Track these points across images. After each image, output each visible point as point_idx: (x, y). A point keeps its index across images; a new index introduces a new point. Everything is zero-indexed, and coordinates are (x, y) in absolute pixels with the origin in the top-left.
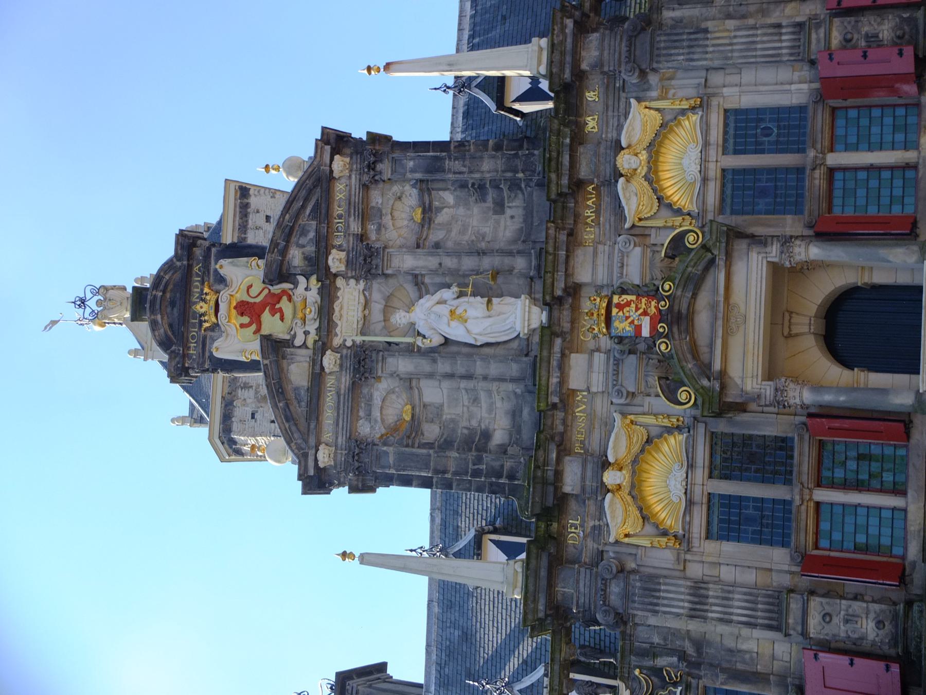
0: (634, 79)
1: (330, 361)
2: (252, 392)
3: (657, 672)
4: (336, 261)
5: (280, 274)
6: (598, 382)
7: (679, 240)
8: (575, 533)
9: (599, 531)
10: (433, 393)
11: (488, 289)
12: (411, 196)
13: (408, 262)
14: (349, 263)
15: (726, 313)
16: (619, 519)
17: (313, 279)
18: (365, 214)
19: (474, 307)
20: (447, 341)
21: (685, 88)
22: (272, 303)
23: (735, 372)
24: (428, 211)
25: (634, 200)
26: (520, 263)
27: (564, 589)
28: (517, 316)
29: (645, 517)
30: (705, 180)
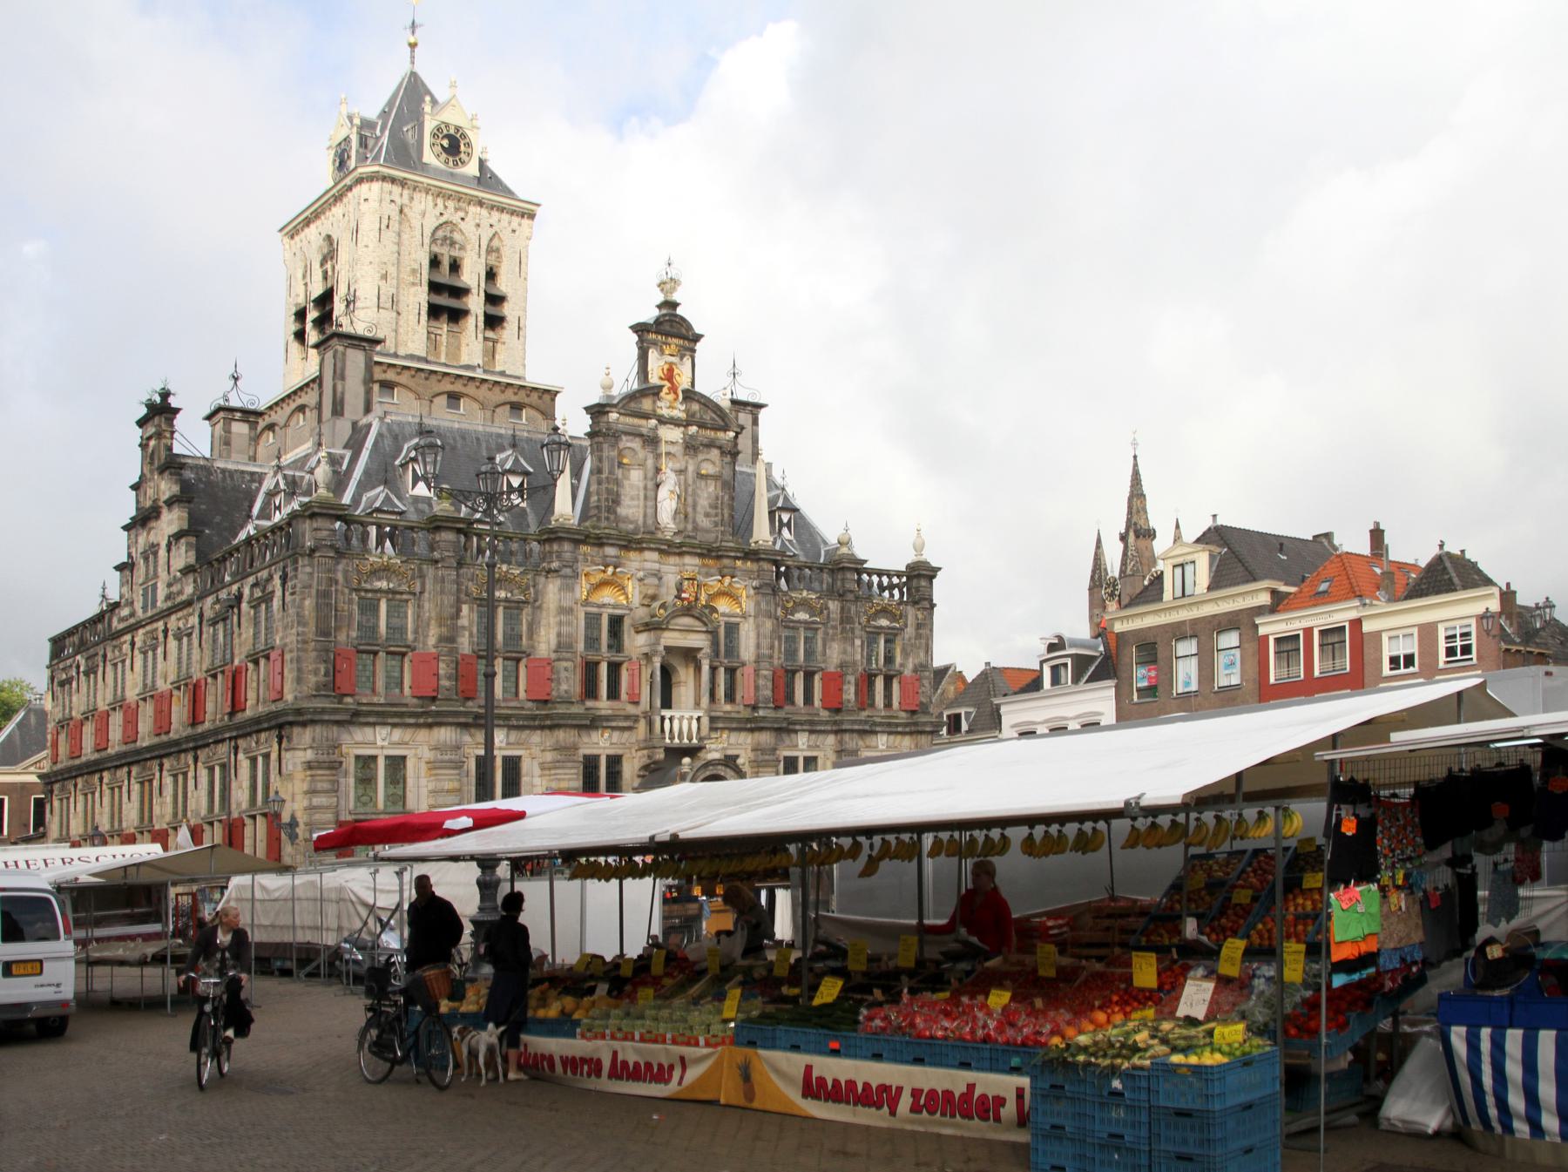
0: (755, 583)
2: (405, 200)
3: (528, 588)
6: (648, 565)
8: (584, 549)
21: (748, 605)
23: (667, 634)
25: (713, 583)
27: (567, 546)
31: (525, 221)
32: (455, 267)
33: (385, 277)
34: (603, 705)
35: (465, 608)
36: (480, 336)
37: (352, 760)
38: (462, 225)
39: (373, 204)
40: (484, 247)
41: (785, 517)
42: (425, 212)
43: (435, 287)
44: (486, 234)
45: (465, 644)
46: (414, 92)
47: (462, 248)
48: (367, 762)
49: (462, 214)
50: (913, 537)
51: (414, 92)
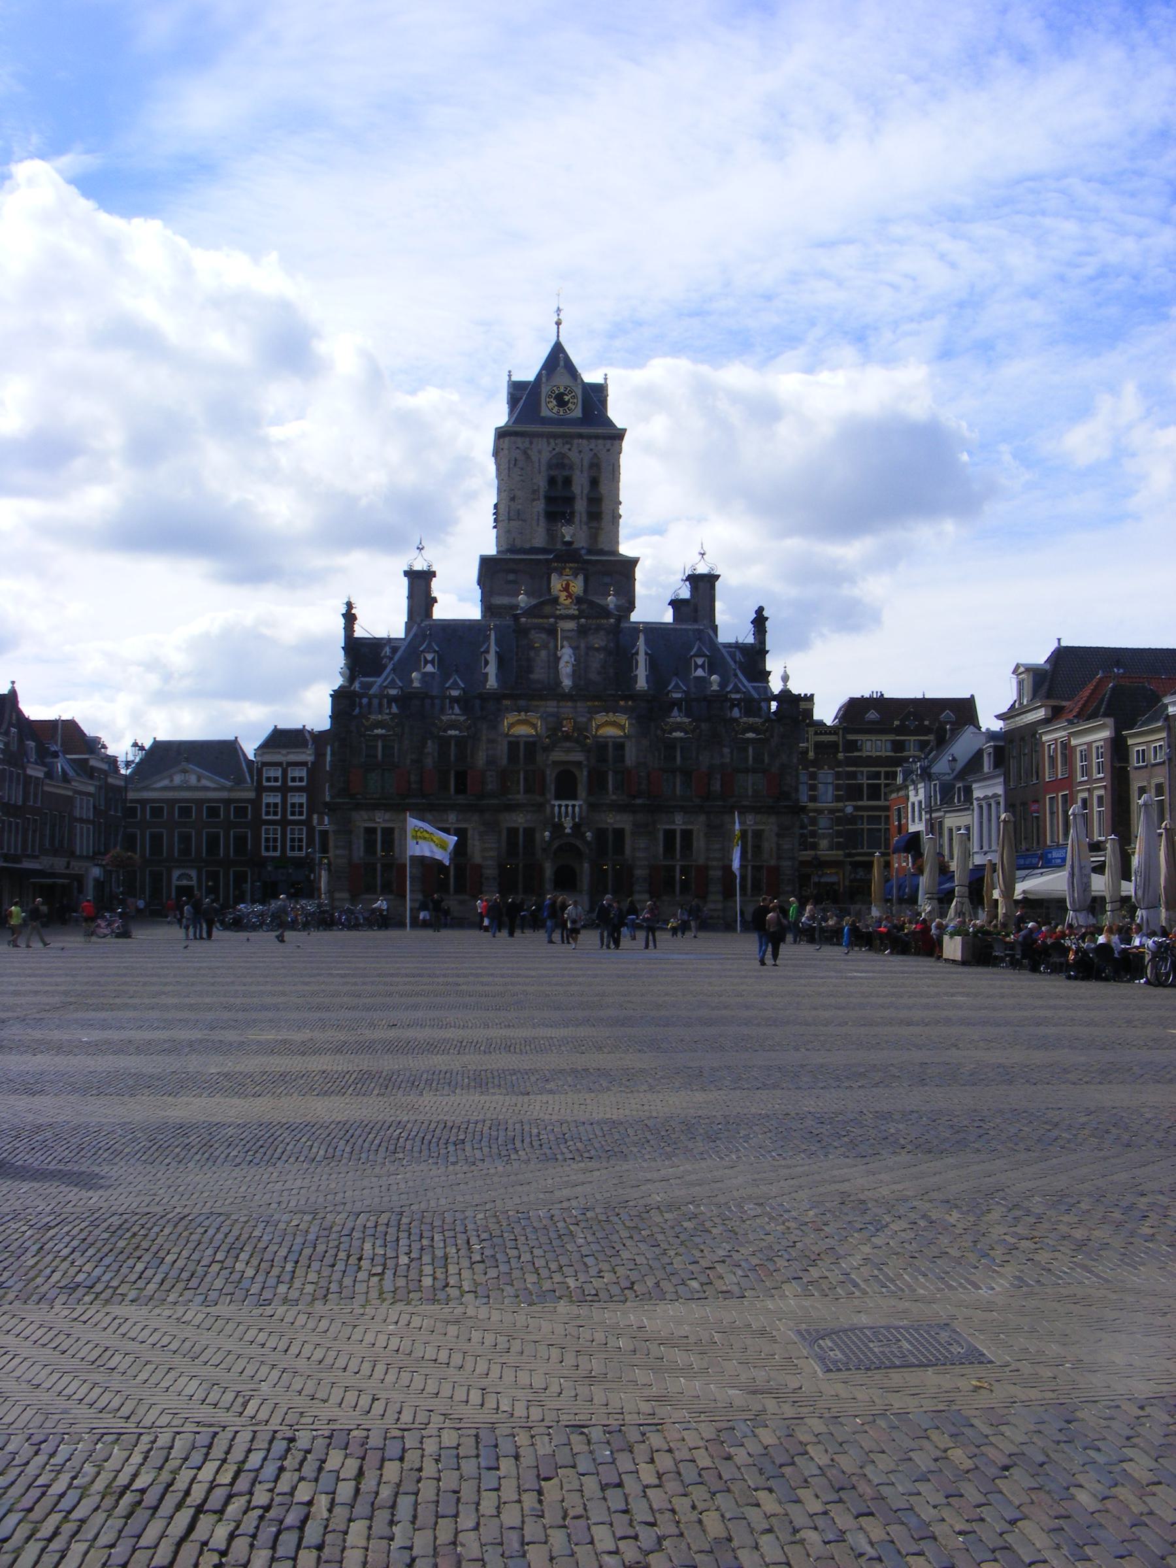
1: (552, 620)
2: (527, 444)
4: (583, 620)
5: (579, 601)
6: (550, 710)
7: (587, 737)
8: (507, 702)
9: (508, 710)
10: (543, 653)
11: (575, 674)
12: (603, 644)
13: (583, 645)
14: (582, 626)
15: (568, 751)
16: (511, 718)
17: (576, 613)
18: (599, 628)
19: (569, 670)
20: (559, 658)
22: (570, 596)
24: (597, 650)
26: (582, 683)
28: (567, 682)
29: (511, 726)
30: (606, 737)
31: (617, 442)
32: (568, 482)
33: (513, 499)
34: (521, 797)
35: (429, 742)
36: (584, 527)
37: (362, 830)
38: (570, 454)
39: (506, 452)
40: (586, 463)
41: (700, 661)
42: (543, 452)
43: (549, 500)
44: (587, 458)
45: (429, 762)
46: (558, 360)
47: (571, 468)
48: (370, 831)
49: (568, 446)
50: (782, 673)
51: (558, 360)
